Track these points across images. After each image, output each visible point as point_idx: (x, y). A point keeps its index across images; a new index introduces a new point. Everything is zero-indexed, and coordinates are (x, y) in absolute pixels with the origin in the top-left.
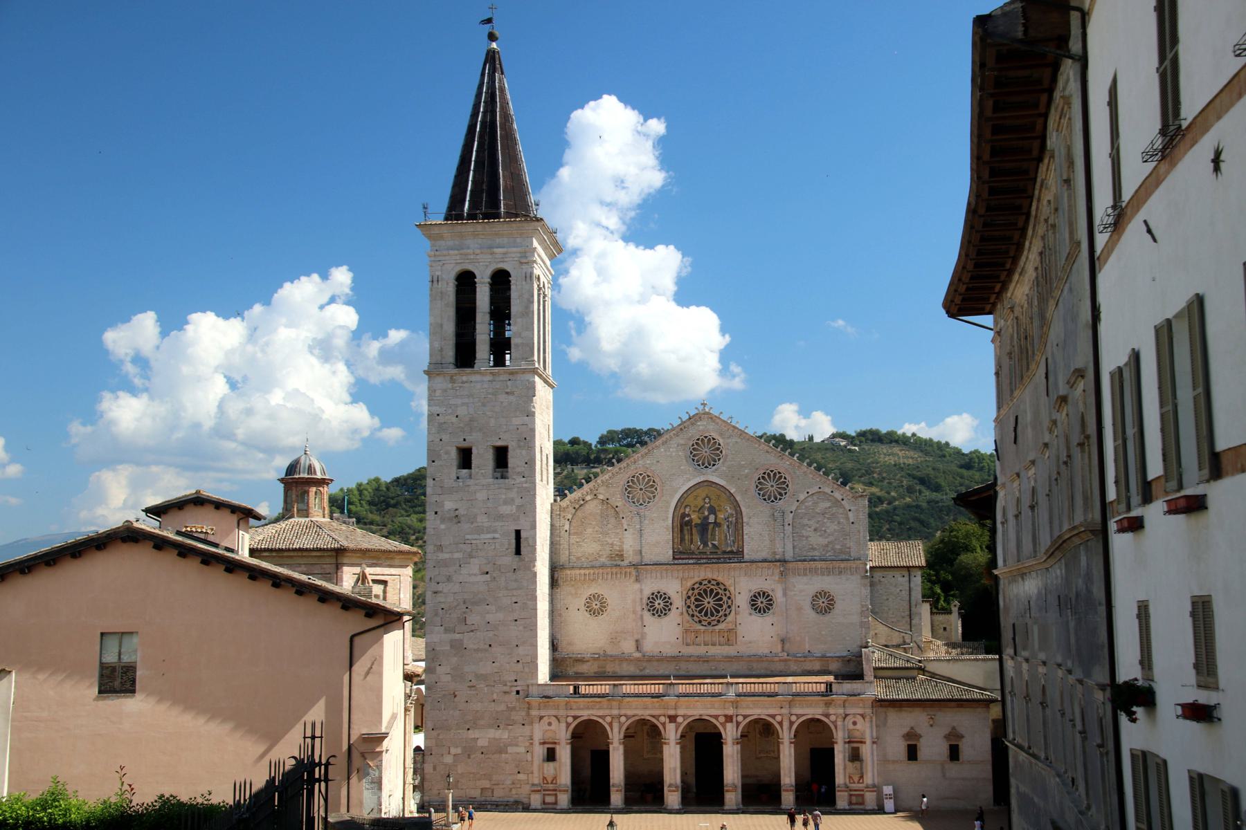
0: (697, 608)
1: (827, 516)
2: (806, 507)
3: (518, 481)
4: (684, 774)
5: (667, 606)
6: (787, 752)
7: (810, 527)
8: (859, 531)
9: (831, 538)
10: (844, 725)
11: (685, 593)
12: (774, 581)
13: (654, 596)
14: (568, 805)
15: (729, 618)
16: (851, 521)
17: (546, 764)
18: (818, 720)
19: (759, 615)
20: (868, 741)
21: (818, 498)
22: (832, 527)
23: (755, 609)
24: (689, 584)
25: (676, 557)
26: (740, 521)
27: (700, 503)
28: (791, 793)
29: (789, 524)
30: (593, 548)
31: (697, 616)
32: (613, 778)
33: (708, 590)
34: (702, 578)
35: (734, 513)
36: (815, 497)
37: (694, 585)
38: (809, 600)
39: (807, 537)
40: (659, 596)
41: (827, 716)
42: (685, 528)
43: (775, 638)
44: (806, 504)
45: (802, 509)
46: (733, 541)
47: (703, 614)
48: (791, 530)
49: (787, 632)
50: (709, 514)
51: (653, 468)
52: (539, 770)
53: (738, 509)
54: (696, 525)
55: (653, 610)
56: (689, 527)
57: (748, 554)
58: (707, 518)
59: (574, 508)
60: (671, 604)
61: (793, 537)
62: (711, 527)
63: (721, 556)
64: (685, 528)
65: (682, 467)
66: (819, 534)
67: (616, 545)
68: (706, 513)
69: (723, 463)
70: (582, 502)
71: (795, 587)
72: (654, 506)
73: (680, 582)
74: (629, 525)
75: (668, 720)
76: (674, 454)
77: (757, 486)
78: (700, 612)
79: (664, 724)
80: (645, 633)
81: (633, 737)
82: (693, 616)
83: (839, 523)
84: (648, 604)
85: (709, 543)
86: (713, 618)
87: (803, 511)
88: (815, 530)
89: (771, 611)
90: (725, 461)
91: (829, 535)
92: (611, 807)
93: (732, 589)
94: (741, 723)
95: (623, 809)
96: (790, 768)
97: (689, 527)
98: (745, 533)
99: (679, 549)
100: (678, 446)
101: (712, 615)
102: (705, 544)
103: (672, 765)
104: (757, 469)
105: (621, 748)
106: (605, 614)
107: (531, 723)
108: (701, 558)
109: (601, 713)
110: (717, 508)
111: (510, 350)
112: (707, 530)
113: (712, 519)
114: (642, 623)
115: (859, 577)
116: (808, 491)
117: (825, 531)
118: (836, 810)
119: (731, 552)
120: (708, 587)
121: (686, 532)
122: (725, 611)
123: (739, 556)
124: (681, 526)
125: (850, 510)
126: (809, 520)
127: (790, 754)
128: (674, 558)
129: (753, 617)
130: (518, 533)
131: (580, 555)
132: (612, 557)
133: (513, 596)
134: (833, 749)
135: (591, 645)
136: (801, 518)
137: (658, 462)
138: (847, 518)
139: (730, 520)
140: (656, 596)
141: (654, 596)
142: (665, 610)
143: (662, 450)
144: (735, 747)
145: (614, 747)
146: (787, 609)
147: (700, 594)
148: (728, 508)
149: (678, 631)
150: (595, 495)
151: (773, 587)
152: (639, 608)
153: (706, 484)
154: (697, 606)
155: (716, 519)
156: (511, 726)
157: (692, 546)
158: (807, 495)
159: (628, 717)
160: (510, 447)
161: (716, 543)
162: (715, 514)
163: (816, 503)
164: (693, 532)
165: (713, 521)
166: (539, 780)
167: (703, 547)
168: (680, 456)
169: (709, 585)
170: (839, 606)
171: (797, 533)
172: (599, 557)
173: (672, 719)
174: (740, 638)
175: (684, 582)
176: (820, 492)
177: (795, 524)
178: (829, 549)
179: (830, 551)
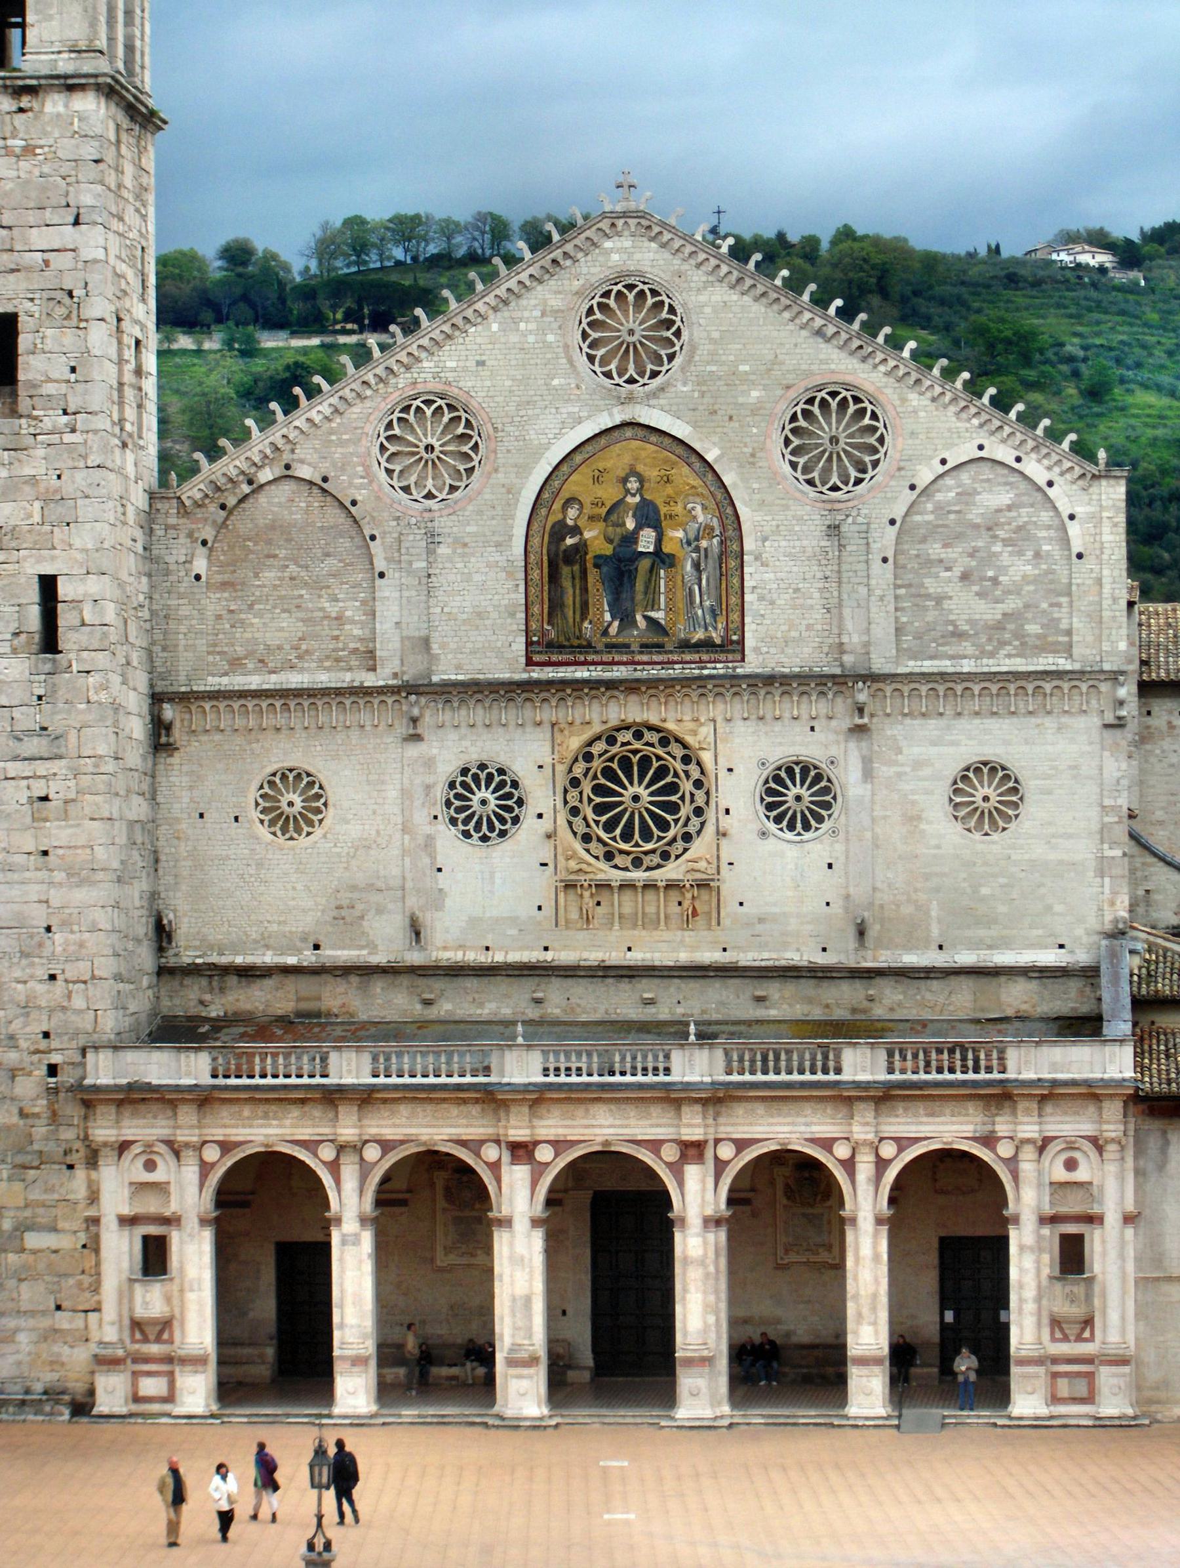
0: (601, 814)
1: (1001, 533)
2: (939, 509)
3: (47, 424)
4: (556, 1312)
5: (509, 809)
6: (866, 1249)
7: (948, 569)
8: (1099, 582)
9: (1012, 604)
10: (1040, 1173)
11: (561, 769)
12: (836, 732)
13: (469, 779)
14: (207, 1405)
15: (699, 848)
16: (1076, 550)
17: (138, 1289)
18: (965, 1154)
19: (789, 835)
20: (1112, 1218)
21: (974, 480)
22: (1018, 568)
23: (778, 820)
24: (575, 743)
25: (536, 658)
26: (735, 547)
27: (609, 493)
28: (877, 1369)
29: (885, 560)
30: (282, 629)
31: (599, 840)
32: (342, 1326)
33: (635, 759)
34: (614, 722)
35: (715, 523)
36: (965, 476)
37: (590, 744)
38: (943, 790)
39: (939, 600)
40: (483, 776)
41: (989, 1141)
43: (837, 908)
44: (939, 497)
46: (713, 611)
47: (618, 832)
48: (890, 576)
49: (874, 889)
50: (639, 527)
51: (467, 384)
52: (120, 1303)
53: (729, 510)
55: (466, 822)
56: (576, 568)
57: (757, 650)
58: (631, 539)
59: (223, 507)
60: (520, 802)
61: (896, 597)
62: (645, 564)
63: (676, 658)
64: (565, 570)
65: (556, 382)
66: (976, 588)
67: (353, 622)
68: (630, 524)
69: (683, 369)
70: (246, 489)
71: (899, 751)
73: (549, 735)
75: (506, 1157)
76: (531, 339)
77: (787, 442)
78: (609, 827)
79: (495, 1167)
80: (441, 890)
81: (403, 1203)
82: (586, 838)
83: (1037, 555)
84: (448, 804)
85: (639, 617)
86: (649, 846)
87: (930, 517)
88: (965, 577)
89: (825, 826)
90: (690, 360)
91: (1009, 592)
92: (336, 1410)
93: (707, 757)
94: (728, 1162)
95: (372, 1416)
96: (875, 1296)
97: (576, 568)
98: (748, 584)
99: (544, 633)
100: (543, 314)
101: (647, 836)
102: (627, 620)
103: (521, 1288)
104: (788, 387)
105: (367, 1239)
106: (318, 832)
107: (92, 1160)
108: (613, 663)
109: (304, 1133)
110: (663, 510)
111: (23, 16)
112: (632, 576)
113: (646, 542)
114: (433, 858)
115: (1096, 721)
116: (945, 455)
117: (995, 581)
118: (1010, 1417)
119: (707, 645)
120: (635, 752)
121: (567, 584)
122: (686, 825)
123: (730, 657)
124: (550, 566)
125: (1072, 517)
126: (945, 546)
127: (876, 1257)
128: (529, 662)
129: (771, 844)
130: (48, 584)
131: (240, 650)
132: (338, 660)
133: (35, 777)
134: (1004, 1241)
135: (274, 927)
136: (924, 540)
137: (480, 363)
138: (1065, 541)
139: (704, 544)
140: (476, 778)
141: (469, 779)
142: (503, 821)
143: (495, 327)
144: (711, 1237)
145: (344, 1235)
146: (873, 820)
147: (608, 773)
148: (699, 508)
149: (543, 885)
150: (288, 467)
151: (834, 751)
152: (421, 817)
153: (629, 433)
154: (600, 809)
155: (659, 541)
156: (32, 1172)
157: (586, 624)
158: (941, 469)
159: (387, 1146)
160: (22, 318)
161: (659, 615)
162: (657, 527)
163: (967, 496)
164: (591, 580)
165: (651, 549)
166: (121, 1330)
167: (621, 629)
168: (548, 346)
169: (637, 745)
170: (1033, 812)
171: (910, 586)
172: (299, 657)
173: (521, 1151)
174: (729, 908)
175: (559, 738)
176: (982, 459)
177: (902, 559)
178: (1007, 636)
179: (1010, 644)
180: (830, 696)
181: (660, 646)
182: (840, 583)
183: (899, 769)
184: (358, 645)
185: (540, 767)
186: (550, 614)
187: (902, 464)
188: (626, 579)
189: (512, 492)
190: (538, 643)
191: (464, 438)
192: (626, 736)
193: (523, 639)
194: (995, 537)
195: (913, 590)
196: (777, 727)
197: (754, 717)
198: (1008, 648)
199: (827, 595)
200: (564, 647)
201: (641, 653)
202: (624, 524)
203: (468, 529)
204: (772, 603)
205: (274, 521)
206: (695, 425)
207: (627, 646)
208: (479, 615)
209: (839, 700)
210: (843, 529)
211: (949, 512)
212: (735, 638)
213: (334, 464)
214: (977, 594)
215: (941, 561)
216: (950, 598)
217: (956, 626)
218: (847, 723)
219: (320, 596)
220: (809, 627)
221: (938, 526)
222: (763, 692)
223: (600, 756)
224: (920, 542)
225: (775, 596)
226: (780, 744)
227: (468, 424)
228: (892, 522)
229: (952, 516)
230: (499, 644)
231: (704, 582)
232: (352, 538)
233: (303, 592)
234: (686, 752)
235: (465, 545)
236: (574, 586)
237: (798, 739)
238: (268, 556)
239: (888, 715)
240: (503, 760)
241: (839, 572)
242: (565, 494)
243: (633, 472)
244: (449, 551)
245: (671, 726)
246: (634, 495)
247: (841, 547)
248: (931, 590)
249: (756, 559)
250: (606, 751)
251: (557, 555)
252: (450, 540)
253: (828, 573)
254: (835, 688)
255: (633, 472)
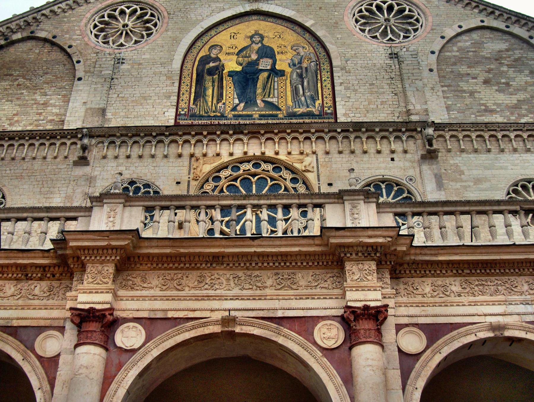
1: (506, 62)
12: (412, 162)
27: (242, 43)
37: (219, 170)
39: (472, 94)
42: (208, 78)
45: (453, 51)
50: (260, 57)
53: (321, 50)
54: (231, 74)
56: (216, 77)
57: (345, 115)
58: (256, 63)
64: (208, 78)
66: (496, 88)
67: (55, 106)
71: (462, 173)
72: (148, 44)
73: (187, 163)
74: (86, 72)
77: (357, 21)
85: (259, 102)
87: (457, 54)
91: (518, 90)
93: (311, 177)
97: (216, 77)
102: (250, 102)
110: (276, 50)
112: (255, 81)
113: (265, 64)
117: (507, 84)
119: (310, 115)
121: (209, 84)
124: (198, 75)
136: (455, 64)
139: (305, 65)
148: (301, 49)
151: (411, 172)
153: (254, 17)
157: (220, 104)
158: (459, 30)
163: (478, 45)
165: (269, 68)
180: (404, 138)
181: (275, 116)
182: (402, 80)
183: (464, 184)
184: (55, 118)
185: (178, 183)
186: (195, 100)
187: (434, 27)
188: (250, 82)
189: (176, 41)
190: (185, 115)
191: (148, 21)
192: (248, 166)
193: (175, 110)
194: (500, 63)
195: (453, 88)
196: (366, 157)
197: (348, 152)
198: (526, 118)
199: (394, 87)
200: (203, 116)
201: (261, 119)
202: (250, 56)
203: (143, 57)
204: (355, 91)
205: (16, 58)
206: (298, 11)
207: (250, 116)
208: (145, 98)
209: (411, 143)
210: (400, 54)
211: (468, 52)
212: (329, 111)
213: (62, 31)
214: (496, 90)
215: (468, 74)
216: (480, 92)
217: (485, 106)
218: (420, 153)
219: (35, 93)
220: (382, 103)
221: (462, 58)
222: (352, 136)
223: (226, 178)
224: (452, 65)
225: (356, 88)
226: (369, 168)
227: (152, 15)
228: (433, 53)
229: (471, 54)
230: (156, 113)
231: (305, 83)
232: (64, 65)
233: (24, 91)
234: (294, 176)
235: (140, 64)
236: (213, 86)
237: (383, 165)
238: (7, 75)
239: (449, 151)
240: (148, 178)
241: (401, 75)
242: (211, 43)
243: (257, 33)
244: (129, 67)
245: (282, 157)
246: (258, 44)
247: (400, 63)
248: (465, 88)
249: (342, 69)
250: (231, 175)
251: (203, 71)
252: (131, 62)
253: (393, 76)
254: (407, 134)
255: (257, 33)
